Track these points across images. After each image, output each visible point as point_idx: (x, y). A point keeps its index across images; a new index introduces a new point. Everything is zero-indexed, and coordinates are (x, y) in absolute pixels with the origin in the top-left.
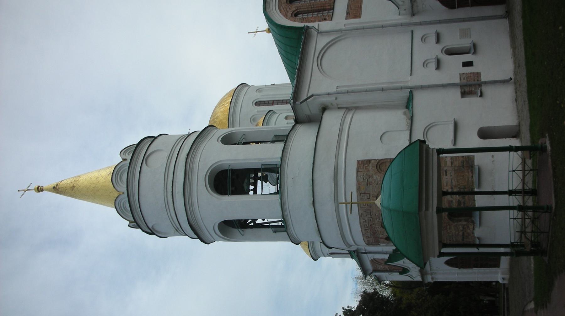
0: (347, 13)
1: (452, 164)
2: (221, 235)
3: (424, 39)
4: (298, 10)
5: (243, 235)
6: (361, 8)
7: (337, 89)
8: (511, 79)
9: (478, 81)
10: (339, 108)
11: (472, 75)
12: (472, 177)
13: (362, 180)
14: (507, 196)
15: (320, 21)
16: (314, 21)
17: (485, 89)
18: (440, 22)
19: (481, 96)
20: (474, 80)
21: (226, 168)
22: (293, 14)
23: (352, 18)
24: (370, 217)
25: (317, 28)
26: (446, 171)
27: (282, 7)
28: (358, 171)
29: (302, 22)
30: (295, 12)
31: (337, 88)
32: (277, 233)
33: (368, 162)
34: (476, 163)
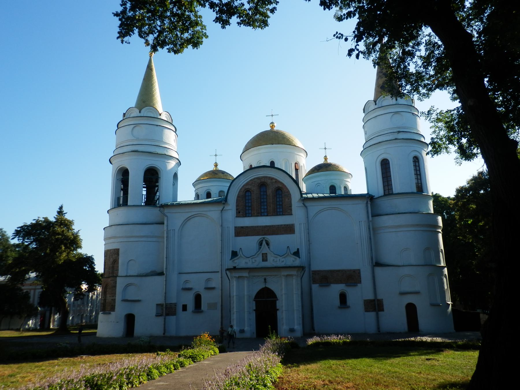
0: (242, 227)
1: (112, 300)
3: (208, 280)
4: (252, 192)
6: (247, 235)
7: (172, 231)
15: (237, 209)
16: (237, 206)
17: (161, 319)
19: (156, 316)
22: (246, 190)
27: (257, 180)
29: (238, 197)
30: (250, 190)
31: (173, 230)
33: (118, 254)
34: (112, 312)
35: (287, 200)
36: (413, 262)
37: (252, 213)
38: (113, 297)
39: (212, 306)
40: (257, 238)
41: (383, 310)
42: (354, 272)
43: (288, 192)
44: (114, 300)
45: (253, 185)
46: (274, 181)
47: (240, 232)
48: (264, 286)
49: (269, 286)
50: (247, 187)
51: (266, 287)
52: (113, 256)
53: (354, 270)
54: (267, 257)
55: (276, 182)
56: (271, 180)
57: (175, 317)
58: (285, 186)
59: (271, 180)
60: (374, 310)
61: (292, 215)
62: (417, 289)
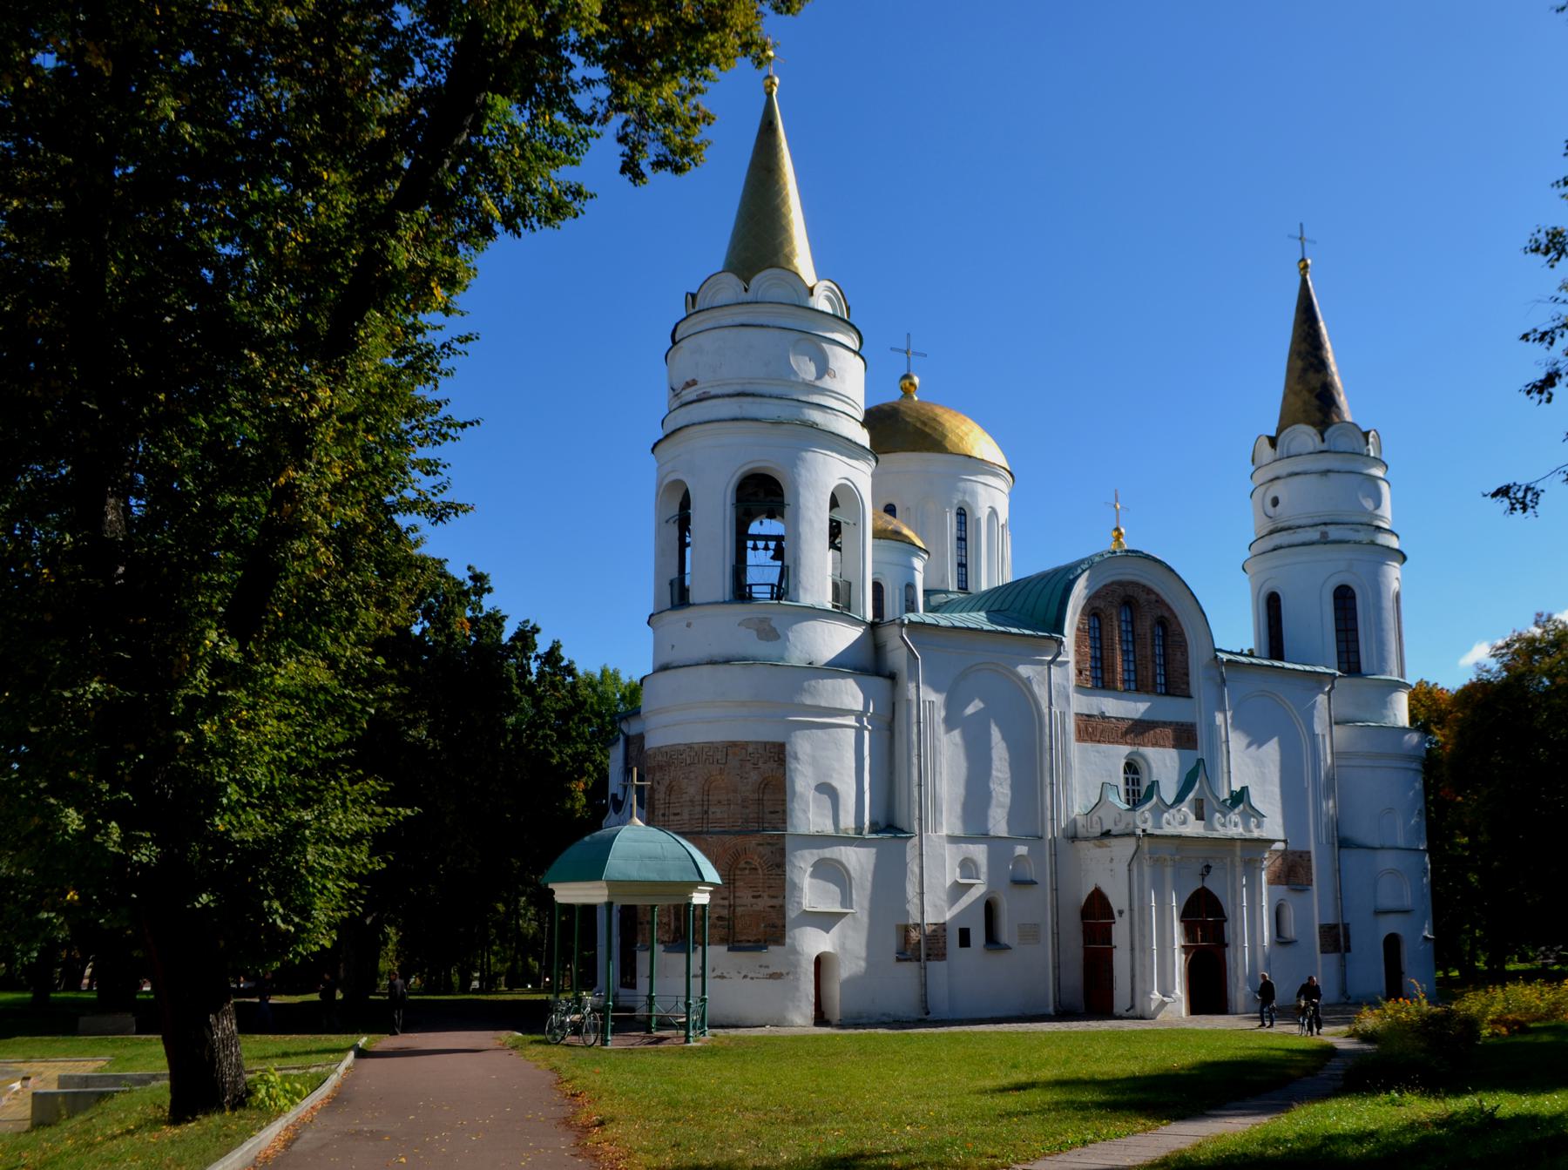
0: (1088, 716)
1: (772, 907)
2: (664, 484)
5: (667, 522)
8: (928, 1013)
9: (928, 955)
10: (894, 704)
11: (941, 945)
12: (749, 941)
13: (750, 750)
14: (647, 993)
15: (1077, 662)
16: (1078, 652)
17: (910, 968)
18: (1055, 890)
19: (898, 960)
20: (930, 949)
21: (788, 498)
22: (1098, 611)
23: (1078, 726)
24: (688, 762)
25: (1059, 659)
26: (759, 896)
28: (765, 744)
29: (1078, 629)
32: (669, 587)
35: (1179, 654)
36: (1401, 843)
37: (1106, 679)
38: (773, 897)
39: (1030, 933)
40: (1120, 753)
41: (1348, 949)
42: (1300, 857)
43: (1182, 634)
44: (781, 910)
45: (1110, 599)
46: (1153, 597)
47: (1092, 729)
48: (1200, 887)
49: (1212, 884)
50: (1097, 603)
51: (1203, 887)
52: (760, 764)
53: (1302, 852)
54: (1202, 808)
55: (1157, 601)
56: (1148, 594)
57: (943, 963)
58: (1176, 617)
59: (1148, 594)
60: (1336, 949)
61: (1189, 697)
62: (1408, 902)
